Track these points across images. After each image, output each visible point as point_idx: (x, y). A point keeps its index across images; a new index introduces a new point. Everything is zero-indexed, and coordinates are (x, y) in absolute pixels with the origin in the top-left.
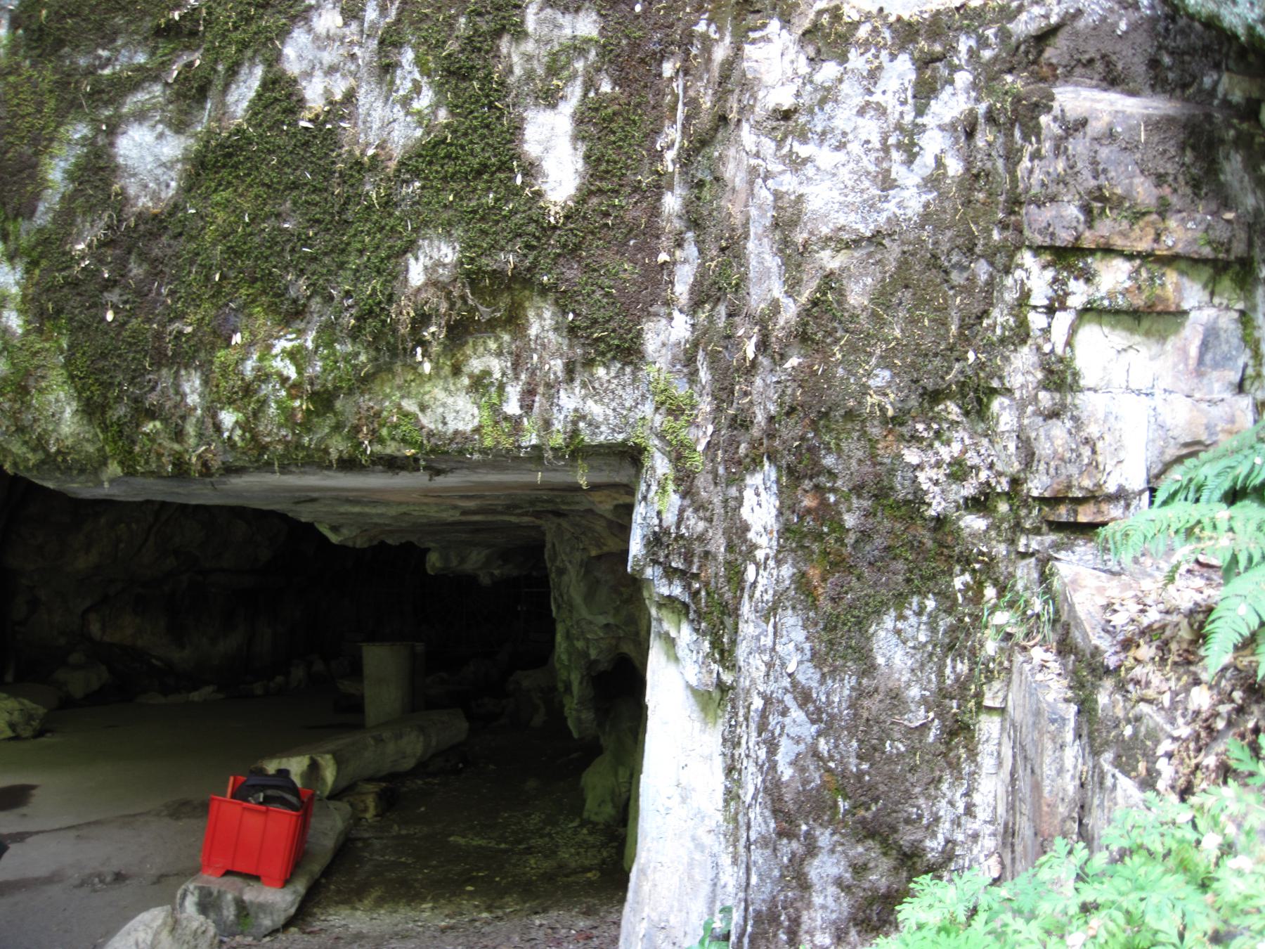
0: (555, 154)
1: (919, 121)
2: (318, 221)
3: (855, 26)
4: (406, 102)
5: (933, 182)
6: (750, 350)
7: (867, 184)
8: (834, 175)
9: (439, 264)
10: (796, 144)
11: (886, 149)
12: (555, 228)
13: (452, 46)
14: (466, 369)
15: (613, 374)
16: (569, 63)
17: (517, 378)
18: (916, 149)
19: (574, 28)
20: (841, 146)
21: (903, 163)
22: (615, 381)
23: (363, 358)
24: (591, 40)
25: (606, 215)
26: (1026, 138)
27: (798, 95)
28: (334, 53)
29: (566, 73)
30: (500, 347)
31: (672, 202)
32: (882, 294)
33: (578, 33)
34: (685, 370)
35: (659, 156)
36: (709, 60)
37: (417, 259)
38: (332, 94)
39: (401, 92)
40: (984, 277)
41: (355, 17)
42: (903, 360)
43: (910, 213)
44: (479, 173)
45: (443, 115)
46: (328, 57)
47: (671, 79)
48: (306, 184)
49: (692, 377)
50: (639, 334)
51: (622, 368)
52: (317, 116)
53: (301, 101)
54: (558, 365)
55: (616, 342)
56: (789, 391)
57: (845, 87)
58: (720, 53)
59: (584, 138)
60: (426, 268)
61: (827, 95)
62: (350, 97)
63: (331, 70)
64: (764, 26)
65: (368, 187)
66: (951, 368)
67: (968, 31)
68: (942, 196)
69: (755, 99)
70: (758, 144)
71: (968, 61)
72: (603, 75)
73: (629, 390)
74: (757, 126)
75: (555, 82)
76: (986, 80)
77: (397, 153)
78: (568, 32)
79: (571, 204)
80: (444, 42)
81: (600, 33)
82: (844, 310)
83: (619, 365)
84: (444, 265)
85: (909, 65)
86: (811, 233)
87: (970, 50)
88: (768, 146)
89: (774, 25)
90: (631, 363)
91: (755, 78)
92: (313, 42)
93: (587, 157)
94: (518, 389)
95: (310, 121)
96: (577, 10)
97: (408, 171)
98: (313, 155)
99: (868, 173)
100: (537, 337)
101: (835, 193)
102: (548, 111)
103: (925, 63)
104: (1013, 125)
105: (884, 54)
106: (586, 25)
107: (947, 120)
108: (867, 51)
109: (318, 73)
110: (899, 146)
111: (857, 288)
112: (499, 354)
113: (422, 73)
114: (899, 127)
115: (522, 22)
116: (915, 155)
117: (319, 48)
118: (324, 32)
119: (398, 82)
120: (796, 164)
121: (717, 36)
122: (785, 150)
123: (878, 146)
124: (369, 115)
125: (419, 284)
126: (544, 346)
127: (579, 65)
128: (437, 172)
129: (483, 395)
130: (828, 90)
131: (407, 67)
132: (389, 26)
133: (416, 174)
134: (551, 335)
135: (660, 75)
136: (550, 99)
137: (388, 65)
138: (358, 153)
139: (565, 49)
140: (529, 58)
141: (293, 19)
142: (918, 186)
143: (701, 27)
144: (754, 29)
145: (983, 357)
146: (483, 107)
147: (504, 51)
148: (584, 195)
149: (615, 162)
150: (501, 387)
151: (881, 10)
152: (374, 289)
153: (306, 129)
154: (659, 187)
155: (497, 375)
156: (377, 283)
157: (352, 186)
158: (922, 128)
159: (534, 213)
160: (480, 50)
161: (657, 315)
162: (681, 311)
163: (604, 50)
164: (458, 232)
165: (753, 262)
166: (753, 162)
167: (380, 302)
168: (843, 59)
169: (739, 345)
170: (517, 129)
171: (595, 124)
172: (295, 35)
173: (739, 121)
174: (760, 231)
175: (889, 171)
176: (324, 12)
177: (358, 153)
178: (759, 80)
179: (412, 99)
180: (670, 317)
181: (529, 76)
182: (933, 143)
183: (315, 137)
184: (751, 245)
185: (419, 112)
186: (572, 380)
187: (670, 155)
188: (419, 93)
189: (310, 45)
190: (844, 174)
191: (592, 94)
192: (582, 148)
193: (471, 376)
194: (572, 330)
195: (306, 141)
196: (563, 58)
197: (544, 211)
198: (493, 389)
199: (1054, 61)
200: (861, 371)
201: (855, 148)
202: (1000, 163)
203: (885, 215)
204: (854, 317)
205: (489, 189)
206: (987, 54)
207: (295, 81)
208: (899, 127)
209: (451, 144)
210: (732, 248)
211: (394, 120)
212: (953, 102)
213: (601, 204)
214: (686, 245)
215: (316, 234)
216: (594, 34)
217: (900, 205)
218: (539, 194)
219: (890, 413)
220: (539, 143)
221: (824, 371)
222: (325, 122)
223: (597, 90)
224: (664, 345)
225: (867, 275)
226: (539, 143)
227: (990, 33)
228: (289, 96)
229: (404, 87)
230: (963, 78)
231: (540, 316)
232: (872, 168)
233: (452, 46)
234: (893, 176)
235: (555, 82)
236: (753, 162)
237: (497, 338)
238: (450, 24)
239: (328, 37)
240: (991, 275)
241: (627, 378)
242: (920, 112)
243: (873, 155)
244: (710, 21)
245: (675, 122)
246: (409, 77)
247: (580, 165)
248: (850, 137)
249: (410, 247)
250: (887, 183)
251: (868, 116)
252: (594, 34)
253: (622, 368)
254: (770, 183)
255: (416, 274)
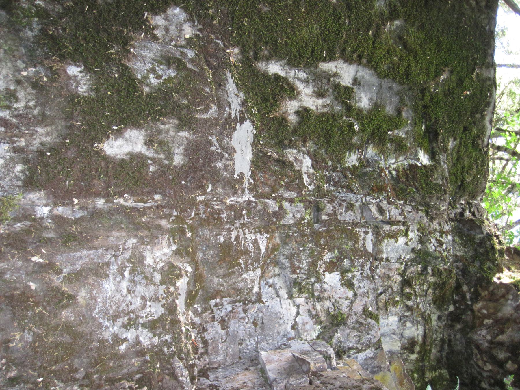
0: (124, 145)
1: (140, 325)
2: (100, 16)
3: (174, 285)
4: (153, 71)
5: (118, 340)
6: (36, 259)
7: (114, 308)
8: (117, 291)
9: (78, 84)
10: (129, 268)
11: (128, 313)
12: (92, 145)
13: (176, 97)
14: (19, 88)
15: (17, 174)
16: (164, 151)
17: (15, 116)
18: (128, 327)
19: (177, 154)
20: (129, 291)
21: (123, 323)
22: (14, 176)
23: (30, 34)
24: (172, 162)
25: (97, 171)
26: (138, 381)
27: (149, 266)
28: (174, 32)
29: (159, 149)
30: (30, 108)
31: (100, 202)
32: (68, 327)
33: (175, 156)
34: (20, 216)
35: (121, 196)
36: (162, 218)
37: (81, 72)
38: (157, 29)
39: (157, 68)
40: (77, 376)
41: (188, 44)
42: (38, 346)
43: (104, 333)
44: (119, 107)
45: (146, 89)
46: (172, 28)
47: (153, 199)
48: (118, 12)
49: (17, 220)
50: (40, 190)
51: (20, 180)
52: (149, 21)
53: (156, 14)
54: (22, 143)
55: (35, 178)
56: (18, 285)
57: (152, 287)
58: (164, 223)
59: (131, 159)
60: (76, 76)
61: (149, 280)
62: (155, 38)
63: (167, 29)
64: (175, 243)
65: (116, 47)
66: (34, 371)
67: (173, 338)
68: (112, 346)
69: (147, 245)
70: (128, 248)
71: (162, 341)
72: (158, 167)
73: (9, 183)
74: (135, 247)
75: (156, 145)
76: (156, 352)
77: (130, 65)
78: (176, 151)
79: (103, 154)
80: (178, 93)
81: (175, 166)
82: (59, 309)
83: (22, 178)
84: (77, 87)
85: (160, 314)
86: (93, 285)
87: (167, 340)
88: (128, 255)
89: (174, 247)
90: (24, 186)
91: (155, 243)
92: (180, 22)
93: (123, 160)
94: (8, 117)
95: (147, 18)
96: (184, 155)
97: (123, 70)
98: (131, 18)
99: (118, 308)
100: (37, 131)
101: (110, 293)
102: (143, 141)
103: (161, 319)
104: (142, 373)
105: (164, 301)
106: (178, 159)
107: (141, 339)
108: (165, 293)
109: (167, 23)
110: (130, 319)
111: (68, 314)
112: (26, 107)
113: (165, 80)
114: (138, 317)
115: (183, 131)
116: (126, 328)
117: (177, 25)
118: (183, 28)
119: (161, 67)
120: (121, 271)
121: (171, 221)
122: (127, 265)
123: (130, 309)
124: (147, 49)
125: (68, 71)
126: (32, 135)
127: (162, 156)
128: (122, 86)
129: (5, 97)
130: (151, 280)
131: (168, 72)
132: (184, 64)
133: (122, 75)
134: (38, 141)
135: (156, 193)
136: (149, 142)
137: (169, 63)
138: (132, 43)
139: (169, 149)
140: (167, 132)
141: (191, 14)
142: (114, 333)
143: (175, 213)
144: (174, 239)
145: (41, 385)
146: (149, 111)
147: (171, 121)
148: (106, 159)
149: (120, 175)
150: (9, 108)
151: (180, 294)
152: (67, 47)
153: (143, 15)
154: (108, 196)
155: (15, 106)
156: (70, 49)
157: (116, 37)
158: (137, 329)
159: (100, 135)
160: (174, 110)
161: (48, 198)
162: (50, 211)
163: (168, 167)
164: (93, 94)
165: (78, 254)
166: (121, 247)
167: (60, 50)
168: (162, 283)
169: (37, 252)
170: (137, 126)
171: (137, 164)
172: (184, 14)
173: (137, 237)
174: (92, 256)
175: (120, 317)
176: (191, 29)
177: (132, 43)
178: (155, 246)
179: (154, 74)
180: (46, 206)
181: (160, 132)
182: (130, 335)
183: (139, 19)
184: (85, 252)
185: (148, 77)
186: (14, 152)
187: (121, 201)
188: (156, 78)
189: (178, 20)
190: (118, 296)
191: (149, 162)
192: (127, 158)
193: (15, 90)
194: (41, 153)
195: (139, 15)
196: (166, 148)
197: (100, 141)
198: (8, 103)
199: (164, 381)
200: (31, 325)
201: (129, 298)
202: (125, 371)
203: (102, 321)
204: (56, 315)
205: (112, 112)
206: (165, 349)
207: (165, 12)
208: (138, 317)
209: (134, 94)
210: (83, 240)
211: (146, 64)
212: (146, 339)
213: (102, 168)
214: (81, 211)
215: (94, 14)
216: (175, 163)
217: (107, 327)
218: (108, 138)
219: (11, 345)
220: (130, 136)
221: (30, 305)
222: (146, 25)
223: (151, 164)
224: (33, 202)
225: (75, 317)
226: (130, 136)
227: (173, 348)
228: (159, 8)
229: (161, 70)
230: (156, 340)
231: (48, 134)
232: (121, 309)
233: (176, 97)
234: (118, 320)
235: (156, 145)
236: (121, 247)
237: (35, 106)
238: (185, 96)
239: (181, 30)
240: (78, 380)
241: (15, 182)
242: (143, 325)
243: (126, 308)
244: (176, 216)
245: (135, 202)
246: (164, 73)
247: (119, 157)
248: (133, 295)
249: (88, 69)
250: (114, 318)
251: (141, 301)
252: (175, 163)
253: (20, 180)
254: (113, 259)
255: (73, 70)
